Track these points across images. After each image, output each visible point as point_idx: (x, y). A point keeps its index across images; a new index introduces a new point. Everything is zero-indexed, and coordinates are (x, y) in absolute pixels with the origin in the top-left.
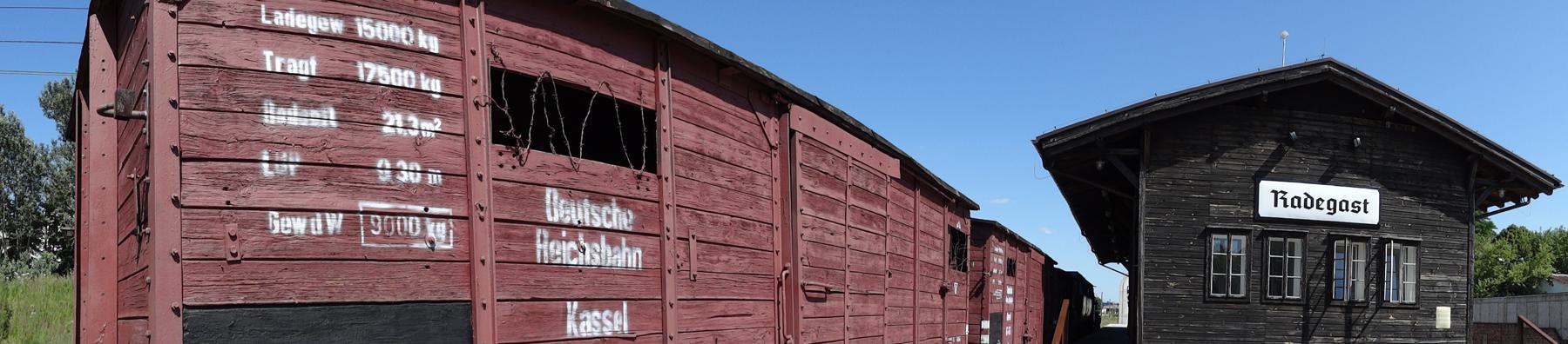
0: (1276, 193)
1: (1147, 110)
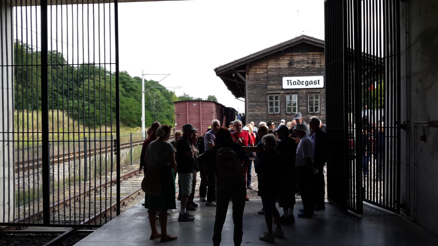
0: (288, 81)
1: (247, 58)
